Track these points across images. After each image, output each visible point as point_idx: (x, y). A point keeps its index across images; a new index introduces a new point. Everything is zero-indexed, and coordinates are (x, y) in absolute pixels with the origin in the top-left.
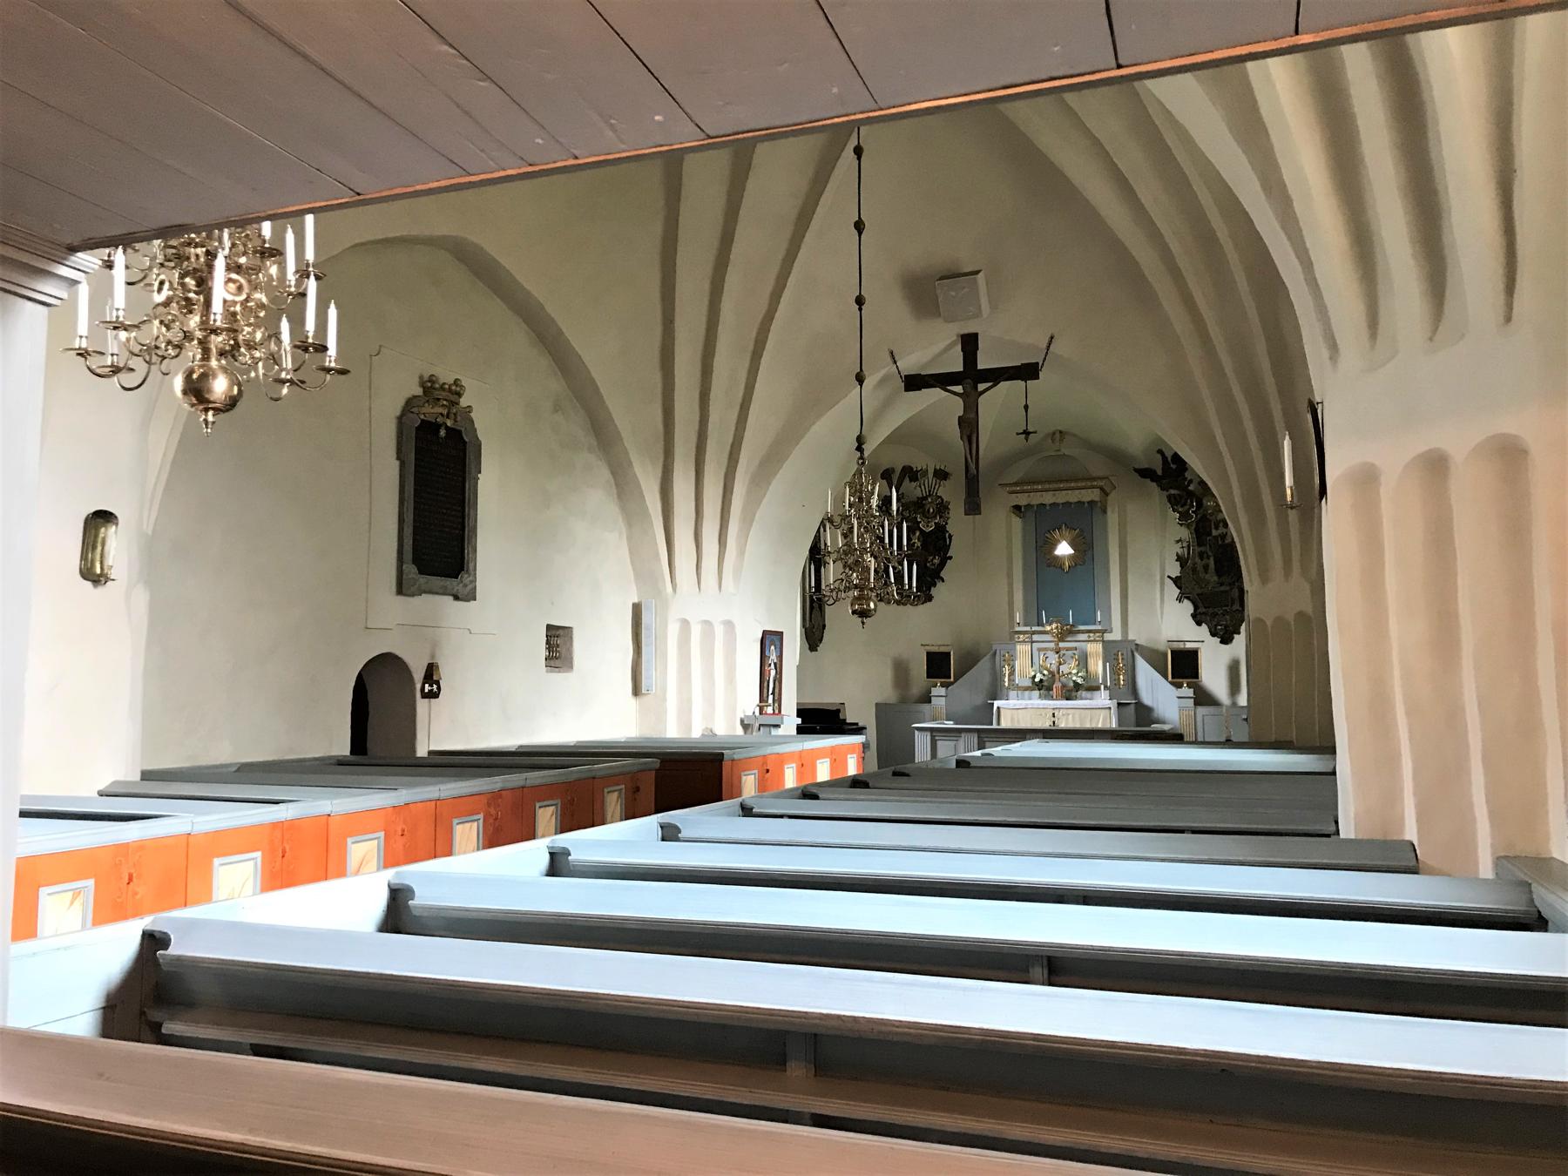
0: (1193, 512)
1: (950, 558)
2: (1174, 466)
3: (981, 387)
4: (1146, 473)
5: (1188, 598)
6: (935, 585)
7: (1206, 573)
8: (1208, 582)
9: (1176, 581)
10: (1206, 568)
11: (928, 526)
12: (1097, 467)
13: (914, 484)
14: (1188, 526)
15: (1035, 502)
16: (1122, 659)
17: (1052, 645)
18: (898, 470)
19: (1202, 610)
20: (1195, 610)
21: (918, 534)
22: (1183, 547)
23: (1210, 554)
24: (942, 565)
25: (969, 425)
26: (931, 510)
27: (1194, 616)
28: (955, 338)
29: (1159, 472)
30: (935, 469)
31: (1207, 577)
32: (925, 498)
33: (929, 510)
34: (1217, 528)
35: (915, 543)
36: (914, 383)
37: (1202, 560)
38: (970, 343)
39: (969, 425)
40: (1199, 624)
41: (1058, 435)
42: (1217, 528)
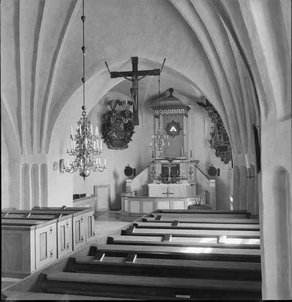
1: (134, 132)
3: (139, 77)
6: (129, 142)
12: (184, 101)
13: (120, 106)
14: (215, 123)
19: (218, 152)
21: (122, 124)
25: (134, 91)
27: (216, 154)
28: (129, 58)
32: (124, 111)
36: (114, 75)
38: (135, 61)
39: (134, 91)
40: (217, 156)
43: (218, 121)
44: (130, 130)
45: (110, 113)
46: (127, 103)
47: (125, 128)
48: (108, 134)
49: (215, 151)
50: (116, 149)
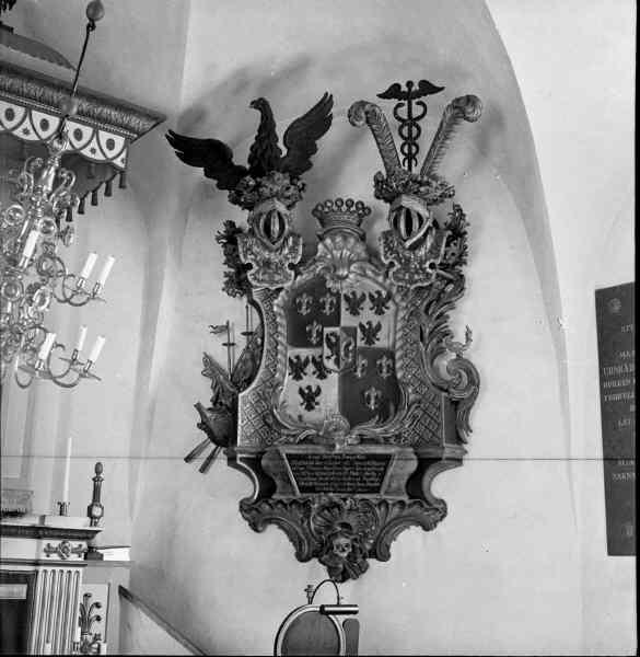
0: (292, 266)
5: (255, 463)
7: (310, 408)
10: (310, 398)
23: (330, 364)
27: (246, 508)
29: (241, 158)
31: (310, 416)
34: (354, 311)
37: (298, 377)
42: (354, 311)
43: (297, 293)
49: (245, 486)
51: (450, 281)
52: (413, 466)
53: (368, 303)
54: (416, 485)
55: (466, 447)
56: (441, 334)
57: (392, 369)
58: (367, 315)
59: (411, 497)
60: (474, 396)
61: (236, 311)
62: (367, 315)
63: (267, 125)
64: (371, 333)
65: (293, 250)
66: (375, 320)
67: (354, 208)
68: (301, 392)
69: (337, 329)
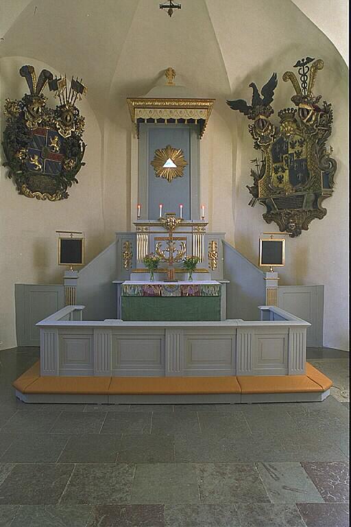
0: (272, 136)
1: (84, 164)
2: (262, 97)
4: (237, 105)
5: (264, 202)
8: (284, 190)
9: (254, 191)
10: (280, 179)
11: (65, 133)
15: (156, 117)
16: (216, 247)
17: (167, 235)
18: (38, 75)
20: (268, 212)
22: (257, 165)
24: (77, 169)
26: (69, 118)
27: (265, 217)
29: (249, 104)
30: (73, 81)
31: (280, 186)
33: (66, 117)
35: (54, 146)
41: (171, 72)
42: (293, 148)
43: (275, 144)
44: (75, 155)
45: (28, 100)
46: (69, 85)
47: (63, 150)
48: (20, 156)
49: (264, 210)
50: (38, 198)
51: (326, 130)
52: (313, 197)
53: (297, 144)
54: (315, 203)
55: (333, 189)
56: (322, 149)
57: (306, 166)
58: (297, 148)
59: (314, 208)
60: (335, 170)
61: (258, 155)
62: (297, 148)
63: (255, 90)
64: (299, 154)
65: (272, 130)
66: (300, 149)
67: (290, 111)
68: (278, 178)
69: (287, 155)
